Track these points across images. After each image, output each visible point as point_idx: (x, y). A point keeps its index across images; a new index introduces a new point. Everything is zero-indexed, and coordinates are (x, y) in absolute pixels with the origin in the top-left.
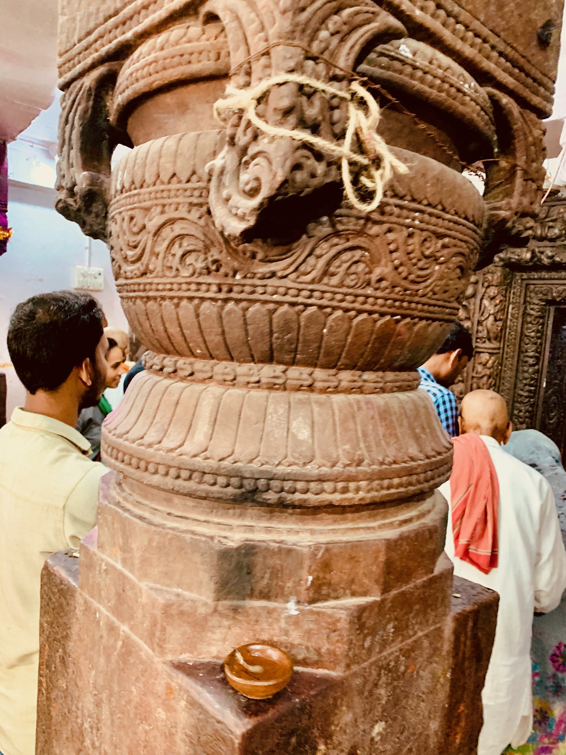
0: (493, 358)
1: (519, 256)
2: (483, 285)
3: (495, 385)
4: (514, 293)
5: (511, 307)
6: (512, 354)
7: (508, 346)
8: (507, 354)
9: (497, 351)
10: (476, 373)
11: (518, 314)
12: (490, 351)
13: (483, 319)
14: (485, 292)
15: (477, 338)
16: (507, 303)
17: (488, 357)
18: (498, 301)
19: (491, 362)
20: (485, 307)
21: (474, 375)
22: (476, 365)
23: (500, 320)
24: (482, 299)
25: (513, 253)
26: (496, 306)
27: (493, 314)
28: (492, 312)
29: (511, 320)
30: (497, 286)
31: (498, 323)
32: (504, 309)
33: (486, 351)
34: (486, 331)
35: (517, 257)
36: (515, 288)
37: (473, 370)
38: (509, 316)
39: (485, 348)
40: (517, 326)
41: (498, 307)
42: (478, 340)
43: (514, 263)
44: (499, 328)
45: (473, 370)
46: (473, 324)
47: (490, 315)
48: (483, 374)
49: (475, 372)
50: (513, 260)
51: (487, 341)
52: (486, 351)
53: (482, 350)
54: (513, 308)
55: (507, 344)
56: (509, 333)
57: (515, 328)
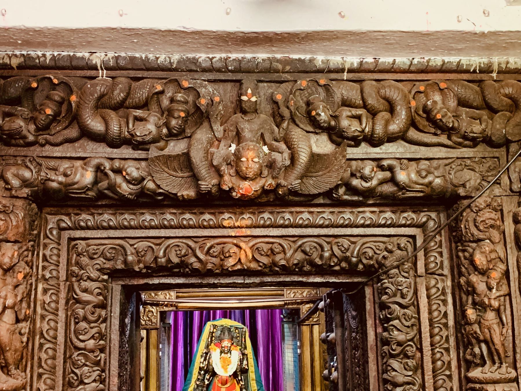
1: (66, 175)
4: (45, 259)
5: (40, 287)
11: (57, 302)
16: (34, 279)
25: (55, 169)
29: (43, 317)
35: (61, 179)
36: (45, 246)
38: (39, 310)
40: (56, 330)
43: (56, 191)
50: (54, 185)
54: (45, 291)
56: (41, 345)
57: (51, 333)
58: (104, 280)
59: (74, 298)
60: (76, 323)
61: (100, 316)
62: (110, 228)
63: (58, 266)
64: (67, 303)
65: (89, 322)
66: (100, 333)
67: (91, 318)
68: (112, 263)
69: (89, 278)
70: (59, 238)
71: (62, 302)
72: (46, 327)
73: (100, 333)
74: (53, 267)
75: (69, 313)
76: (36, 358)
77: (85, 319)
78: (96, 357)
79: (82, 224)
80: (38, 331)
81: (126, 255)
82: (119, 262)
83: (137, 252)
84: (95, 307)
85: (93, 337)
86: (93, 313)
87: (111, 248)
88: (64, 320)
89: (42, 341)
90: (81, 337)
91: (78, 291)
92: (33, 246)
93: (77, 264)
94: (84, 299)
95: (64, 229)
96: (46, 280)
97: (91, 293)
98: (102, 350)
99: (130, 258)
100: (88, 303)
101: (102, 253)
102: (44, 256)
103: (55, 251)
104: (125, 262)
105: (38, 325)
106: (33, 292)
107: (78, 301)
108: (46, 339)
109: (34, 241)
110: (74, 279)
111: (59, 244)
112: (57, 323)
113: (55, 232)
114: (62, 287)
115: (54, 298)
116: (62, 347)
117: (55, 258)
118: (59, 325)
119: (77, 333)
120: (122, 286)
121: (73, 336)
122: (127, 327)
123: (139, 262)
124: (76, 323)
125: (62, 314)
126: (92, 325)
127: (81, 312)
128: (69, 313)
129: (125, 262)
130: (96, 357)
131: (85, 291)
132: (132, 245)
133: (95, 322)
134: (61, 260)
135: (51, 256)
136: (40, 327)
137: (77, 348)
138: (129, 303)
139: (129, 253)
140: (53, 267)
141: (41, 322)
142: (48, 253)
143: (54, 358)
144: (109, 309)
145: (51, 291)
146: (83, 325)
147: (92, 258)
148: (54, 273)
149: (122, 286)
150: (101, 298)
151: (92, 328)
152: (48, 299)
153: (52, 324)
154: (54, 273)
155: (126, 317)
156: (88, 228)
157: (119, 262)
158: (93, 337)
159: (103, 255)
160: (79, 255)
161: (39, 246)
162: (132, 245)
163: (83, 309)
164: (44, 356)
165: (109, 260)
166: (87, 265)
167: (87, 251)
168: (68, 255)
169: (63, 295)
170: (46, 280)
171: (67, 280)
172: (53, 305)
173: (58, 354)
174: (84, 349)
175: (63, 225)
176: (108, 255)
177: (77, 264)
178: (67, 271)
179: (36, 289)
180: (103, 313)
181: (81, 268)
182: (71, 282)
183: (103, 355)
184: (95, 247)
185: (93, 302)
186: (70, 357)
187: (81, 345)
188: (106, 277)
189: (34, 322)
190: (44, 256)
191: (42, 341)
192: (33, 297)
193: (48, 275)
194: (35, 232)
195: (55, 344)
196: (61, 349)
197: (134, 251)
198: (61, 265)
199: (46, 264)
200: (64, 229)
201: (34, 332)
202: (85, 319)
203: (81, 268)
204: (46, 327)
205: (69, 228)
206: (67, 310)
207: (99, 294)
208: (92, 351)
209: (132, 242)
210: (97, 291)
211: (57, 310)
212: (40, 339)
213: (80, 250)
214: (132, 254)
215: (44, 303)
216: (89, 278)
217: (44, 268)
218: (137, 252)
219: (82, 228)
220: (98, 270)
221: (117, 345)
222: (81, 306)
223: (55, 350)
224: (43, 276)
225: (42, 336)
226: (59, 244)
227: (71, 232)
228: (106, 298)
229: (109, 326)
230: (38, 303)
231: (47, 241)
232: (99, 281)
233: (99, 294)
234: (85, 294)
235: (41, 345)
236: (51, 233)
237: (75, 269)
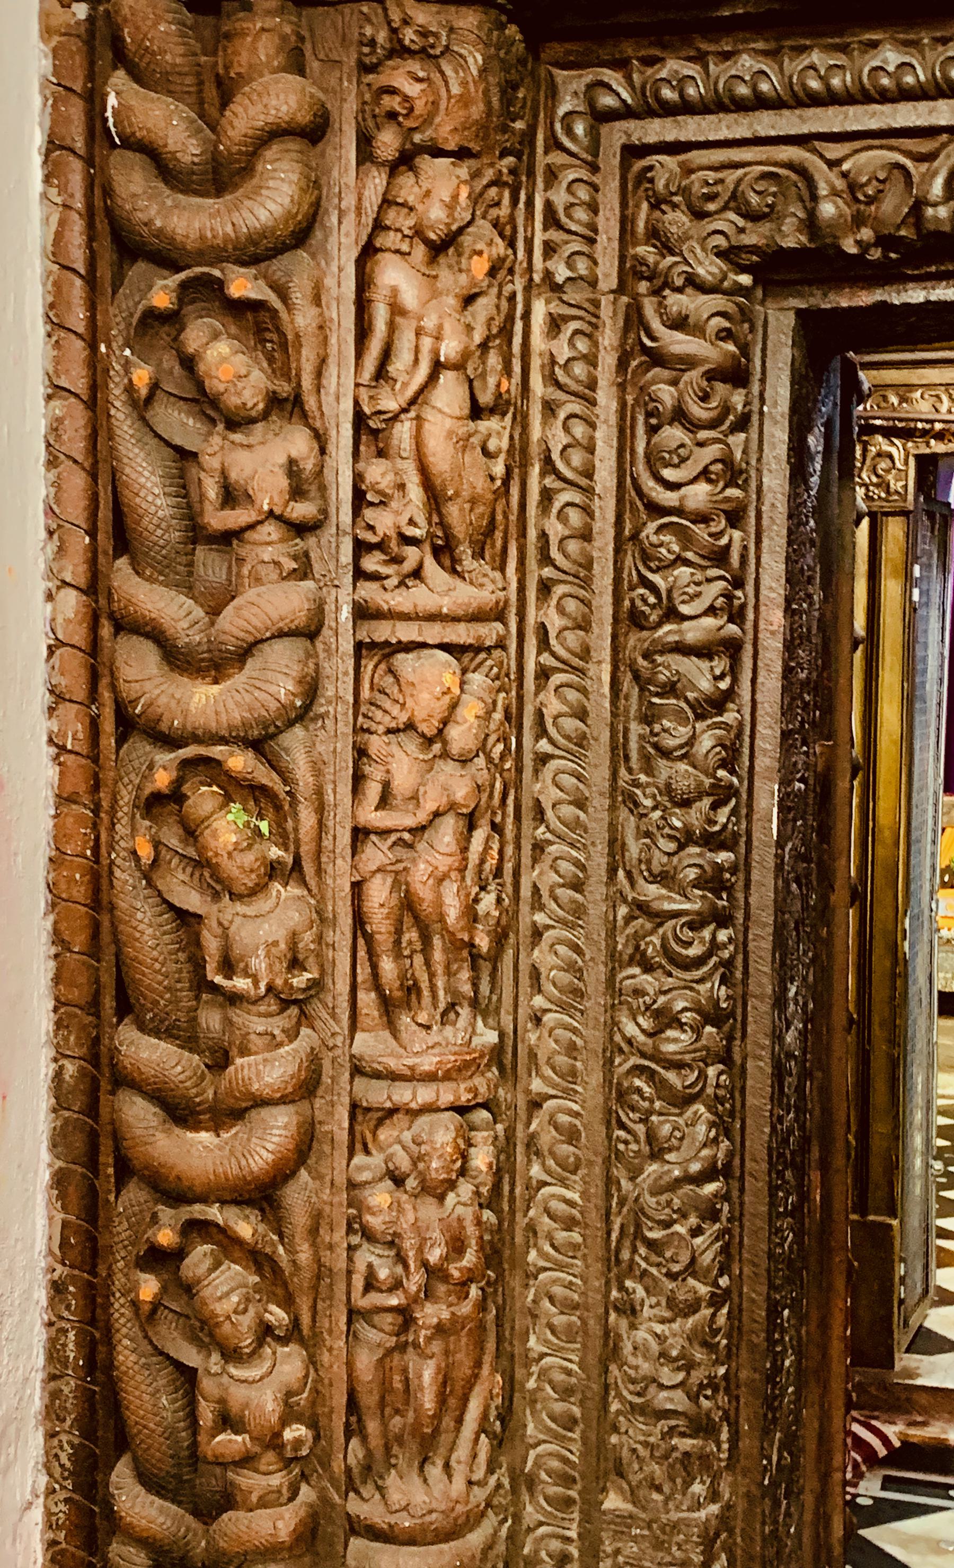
0: (477, 679)
2: (365, 142)
3: (498, 872)
4: (551, 220)
5: (540, 310)
6: (573, 639)
7: (545, 588)
8: (544, 644)
9: (489, 632)
10: (384, 801)
11: (591, 360)
12: (461, 634)
13: (390, 404)
14: (387, 202)
15: (361, 548)
16: (519, 285)
17: (450, 679)
18: (480, 266)
19: (470, 711)
20: (397, 310)
21: (371, 816)
22: (376, 744)
23: (498, 408)
24: (369, 252)
26: (469, 300)
27: (459, 366)
28: (450, 348)
29: (550, 408)
30: (461, 154)
31: (484, 425)
32: (506, 332)
33: (434, 633)
34: (415, 493)
36: (552, 175)
37: (358, 779)
39: (434, 617)
41: (484, 307)
42: (371, 563)
44: (499, 469)
45: (358, 779)
46: (321, 440)
47: (437, 367)
48: (430, 805)
49: (373, 791)
51: (430, 565)
52: (434, 633)
53: (406, 632)
54: (555, 324)
55: (535, 573)
56: (547, 496)
57: (577, 458)
58: (739, 290)
59: (645, 350)
60: (652, 430)
61: (726, 409)
62: (760, 103)
63: (591, 241)
64: (622, 365)
65: (693, 426)
66: (726, 460)
67: (698, 411)
68: (765, 228)
69: (693, 283)
70: (594, 146)
71: (608, 360)
72: (558, 440)
73: (726, 460)
74: (576, 246)
75: (630, 399)
76: (532, 534)
77: (680, 415)
78: (717, 535)
79: (668, 93)
80: (535, 450)
81: (814, 198)
82: (789, 225)
83: (853, 187)
84: (711, 376)
85: (704, 474)
86: (705, 398)
87: (764, 176)
88: (613, 420)
89: (549, 481)
90: (668, 474)
91: (656, 325)
92: (513, 171)
93: (655, 235)
94: (677, 349)
95: (610, 116)
96: (557, 288)
97: (698, 330)
98: (735, 518)
99: (827, 209)
100: (689, 362)
101: (734, 196)
102: (549, 207)
103: (583, 193)
104: (811, 223)
105: (536, 432)
106: (519, 326)
107: (657, 358)
108: (560, 477)
109: (519, 158)
110: (643, 287)
111: (594, 168)
112: (593, 426)
113: (580, 129)
114: (606, 311)
115: (582, 345)
116: (611, 503)
117: (581, 214)
118: (598, 434)
119: (654, 461)
120: (799, 313)
121: (641, 468)
122: (812, 459)
123: (859, 221)
124: (652, 430)
125: (606, 399)
126: (703, 435)
127: (666, 394)
128: (630, 399)
129: (811, 223)
130: (717, 535)
131: (680, 323)
132: (833, 164)
133: (713, 424)
134: (601, 221)
135: (569, 207)
136: (544, 440)
137: (656, 510)
138: (819, 382)
139: (823, 191)
140: (576, 246)
141: (544, 423)
142: (560, 198)
143: (586, 536)
144: (756, 388)
145: (573, 325)
146: (673, 435)
147: (699, 215)
148: (582, 266)
149: (799, 313)
150: (731, 347)
151: (701, 444)
152: (563, 354)
153: (579, 429)
154: (582, 266)
155: (809, 430)
156: (686, 108)
157: (789, 225)
158: (704, 474)
159: (736, 202)
160: (655, 206)
161: (531, 174)
162: (833, 164)
163: (674, 383)
164: (555, 529)
165: (754, 217)
166: (685, 238)
167: (685, 191)
168: (624, 204)
169: (609, 338)
170: (557, 288)
171: (620, 290)
172: (579, 369)
173: (597, 526)
174: (679, 511)
175: (607, 101)
176: (754, 199)
177: (655, 235)
178: (622, 258)
179: (526, 316)
180: (738, 399)
181: (667, 248)
182: (636, 297)
183: (737, 534)
184: (711, 176)
185: (705, 361)
186: (635, 537)
187: (668, 498)
188: (745, 279)
189: (522, 421)
190: (549, 207)
191: (549, 481)
192: (517, 340)
193: (562, 273)
194: (519, 125)
195: (589, 491)
196: (605, 509)
197: (840, 184)
198: (602, 239)
199: (555, 235)
200: (610, 116)
201: (524, 450)
202: (680, 415)
203: (667, 248)
204: (558, 440)
205: (626, 113)
206: (622, 387)
207: (725, 335)
208: (703, 518)
209: (834, 151)
210: (718, 322)
211: (592, 385)
212: (543, 474)
213: (660, 185)
214: (835, 193)
215: (553, 362)
216: (693, 283)
217: (550, 249)
218: (853, 187)
219: (668, 110)
220: (720, 254)
221: (782, 508)
222: (666, 374)
223: (587, 511)
224: (548, 275)
225: (548, 466)
226: (594, 168)
227: (630, 124)
228: (745, 349)
229: (754, 445)
230: (536, 363)
231: (557, 158)
232: (725, 293)
233: (725, 335)
234: (679, 336)
235: (547, 496)
236: (569, 132)
237: (643, 250)
